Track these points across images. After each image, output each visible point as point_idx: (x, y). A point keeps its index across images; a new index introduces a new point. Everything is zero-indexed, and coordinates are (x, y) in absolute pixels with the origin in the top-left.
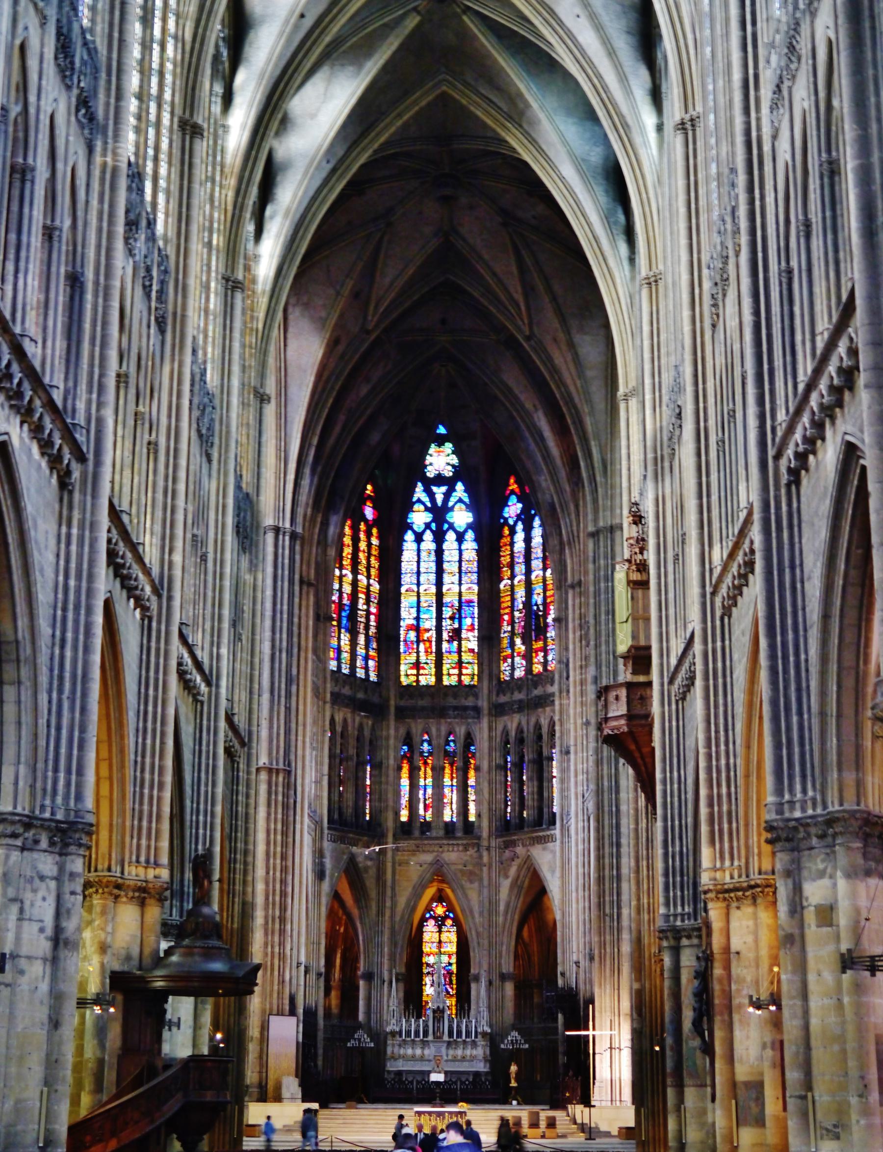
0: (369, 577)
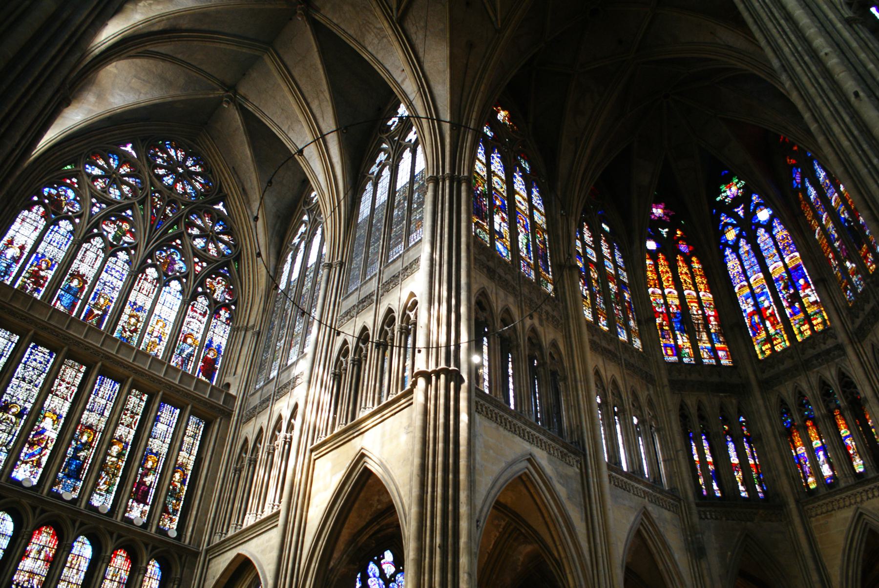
0: (697, 291)
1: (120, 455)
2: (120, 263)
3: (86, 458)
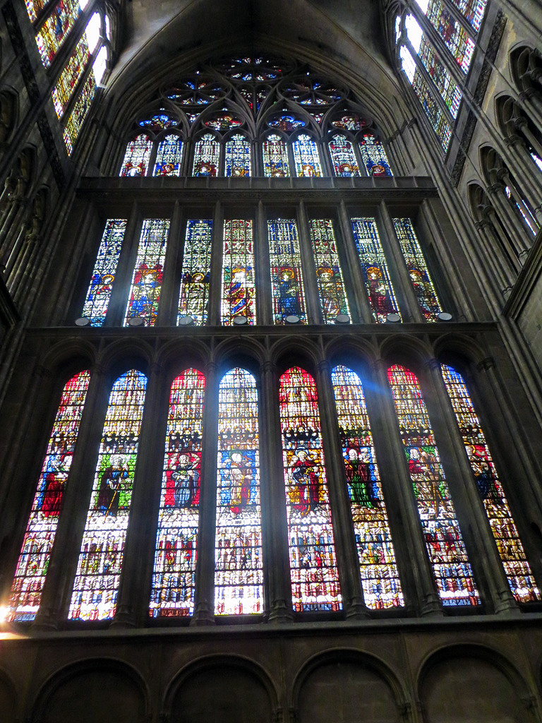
1: (334, 279)
2: (239, 143)
3: (297, 293)
